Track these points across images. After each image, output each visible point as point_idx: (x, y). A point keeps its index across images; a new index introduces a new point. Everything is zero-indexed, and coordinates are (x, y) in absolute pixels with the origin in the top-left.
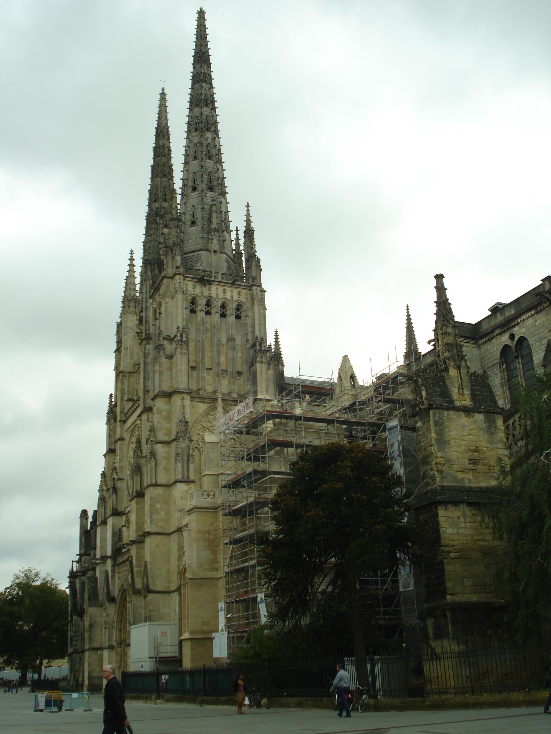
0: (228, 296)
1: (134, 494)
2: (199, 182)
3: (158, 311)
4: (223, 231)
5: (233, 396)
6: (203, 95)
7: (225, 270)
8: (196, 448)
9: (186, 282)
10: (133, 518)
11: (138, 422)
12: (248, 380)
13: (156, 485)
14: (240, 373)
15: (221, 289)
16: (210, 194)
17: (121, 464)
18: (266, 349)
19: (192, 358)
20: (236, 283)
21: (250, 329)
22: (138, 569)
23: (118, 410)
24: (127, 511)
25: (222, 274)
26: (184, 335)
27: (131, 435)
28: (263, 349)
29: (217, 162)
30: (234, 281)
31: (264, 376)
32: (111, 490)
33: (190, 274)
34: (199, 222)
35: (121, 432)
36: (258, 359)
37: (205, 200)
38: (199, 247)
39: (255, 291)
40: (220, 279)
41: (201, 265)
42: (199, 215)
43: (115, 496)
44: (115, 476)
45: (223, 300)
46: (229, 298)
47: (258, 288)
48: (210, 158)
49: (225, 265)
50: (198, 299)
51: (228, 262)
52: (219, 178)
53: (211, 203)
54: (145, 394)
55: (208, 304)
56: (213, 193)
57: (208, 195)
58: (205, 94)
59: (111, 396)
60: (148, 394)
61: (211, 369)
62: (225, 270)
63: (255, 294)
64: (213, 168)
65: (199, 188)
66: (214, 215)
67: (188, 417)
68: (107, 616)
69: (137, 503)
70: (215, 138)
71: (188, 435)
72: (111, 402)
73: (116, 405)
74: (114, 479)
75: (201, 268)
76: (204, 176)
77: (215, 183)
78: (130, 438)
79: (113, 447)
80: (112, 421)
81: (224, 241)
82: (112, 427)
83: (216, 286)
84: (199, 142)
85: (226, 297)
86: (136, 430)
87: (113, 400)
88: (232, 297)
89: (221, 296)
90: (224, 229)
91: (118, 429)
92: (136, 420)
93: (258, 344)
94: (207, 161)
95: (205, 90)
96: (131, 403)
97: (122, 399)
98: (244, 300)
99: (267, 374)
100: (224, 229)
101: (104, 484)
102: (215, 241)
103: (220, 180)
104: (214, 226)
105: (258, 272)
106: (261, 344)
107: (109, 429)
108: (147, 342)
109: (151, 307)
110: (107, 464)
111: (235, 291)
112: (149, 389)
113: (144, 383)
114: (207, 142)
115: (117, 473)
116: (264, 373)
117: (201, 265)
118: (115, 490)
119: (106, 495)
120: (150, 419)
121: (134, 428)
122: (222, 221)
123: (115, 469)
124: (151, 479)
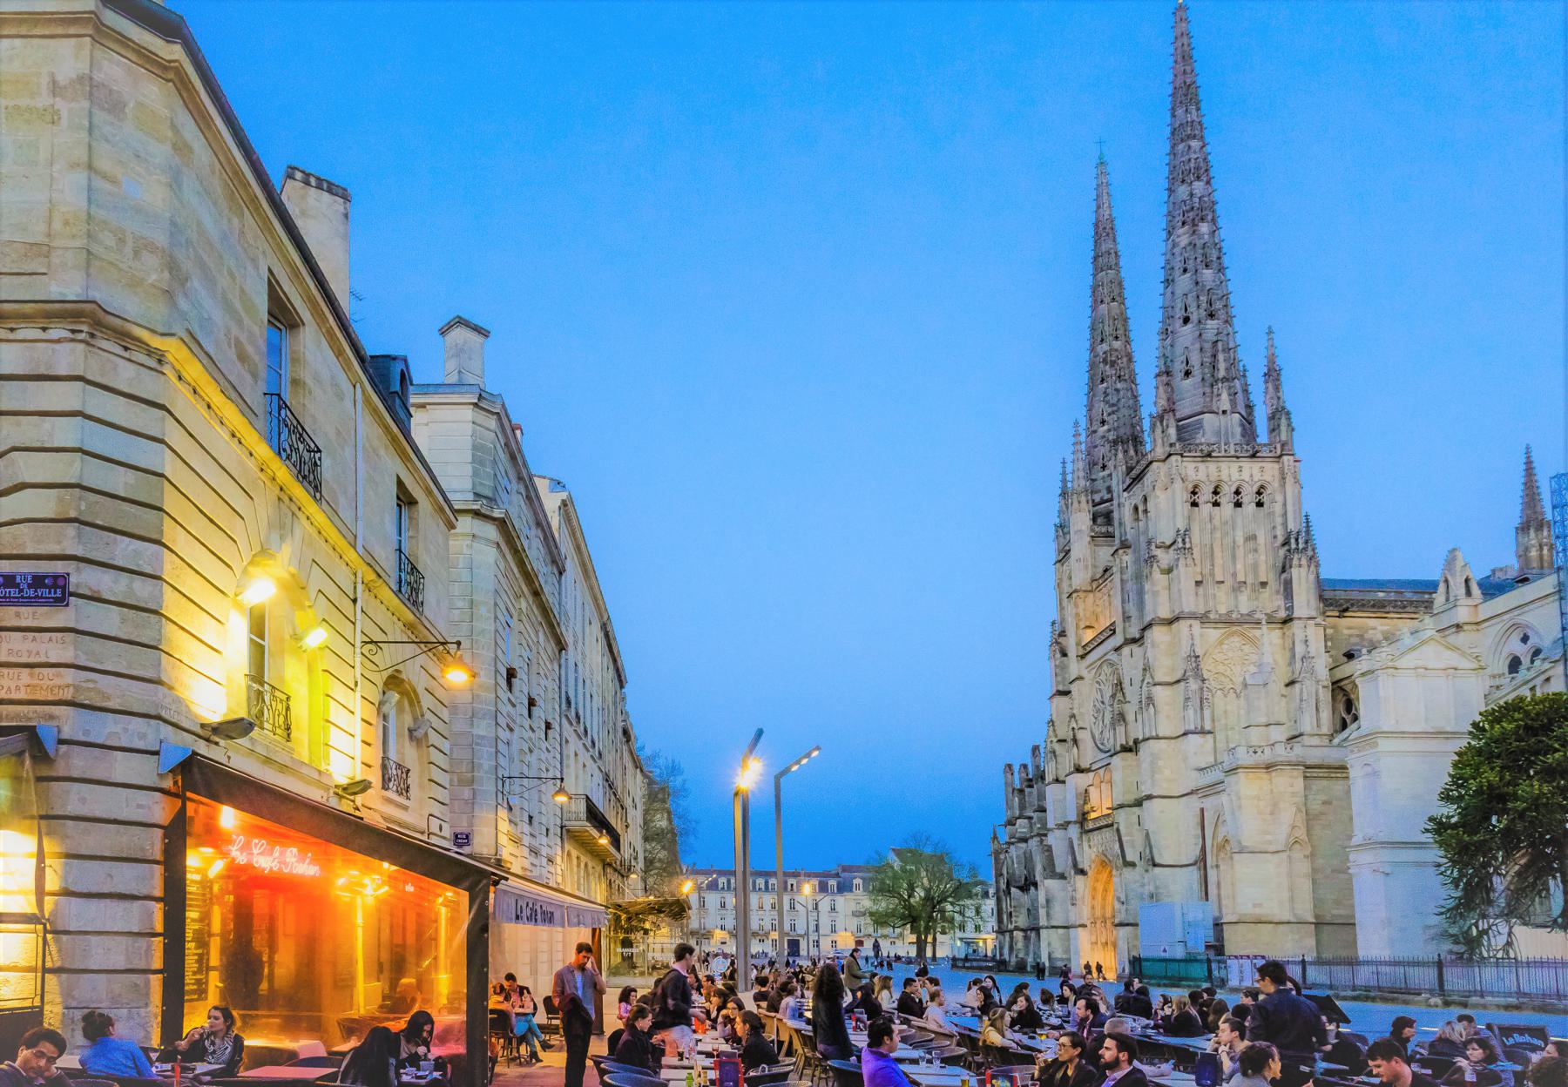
0: (1246, 475)
2: (1192, 309)
5: (1256, 616)
6: (1193, 161)
12: (1278, 592)
13: (1158, 738)
14: (1264, 584)
15: (1234, 466)
16: (1211, 324)
21: (1279, 520)
34: (1196, 371)
37: (1204, 336)
38: (1198, 409)
42: (1195, 360)
50: (1202, 485)
53: (1215, 339)
57: (1208, 327)
58: (1196, 159)
61: (1223, 582)
64: (1214, 281)
65: (1194, 318)
66: (1221, 357)
75: (1203, 440)
76: (1201, 298)
84: (1190, 244)
94: (1204, 271)
114: (1202, 241)
117: (1203, 436)
124: (1150, 731)
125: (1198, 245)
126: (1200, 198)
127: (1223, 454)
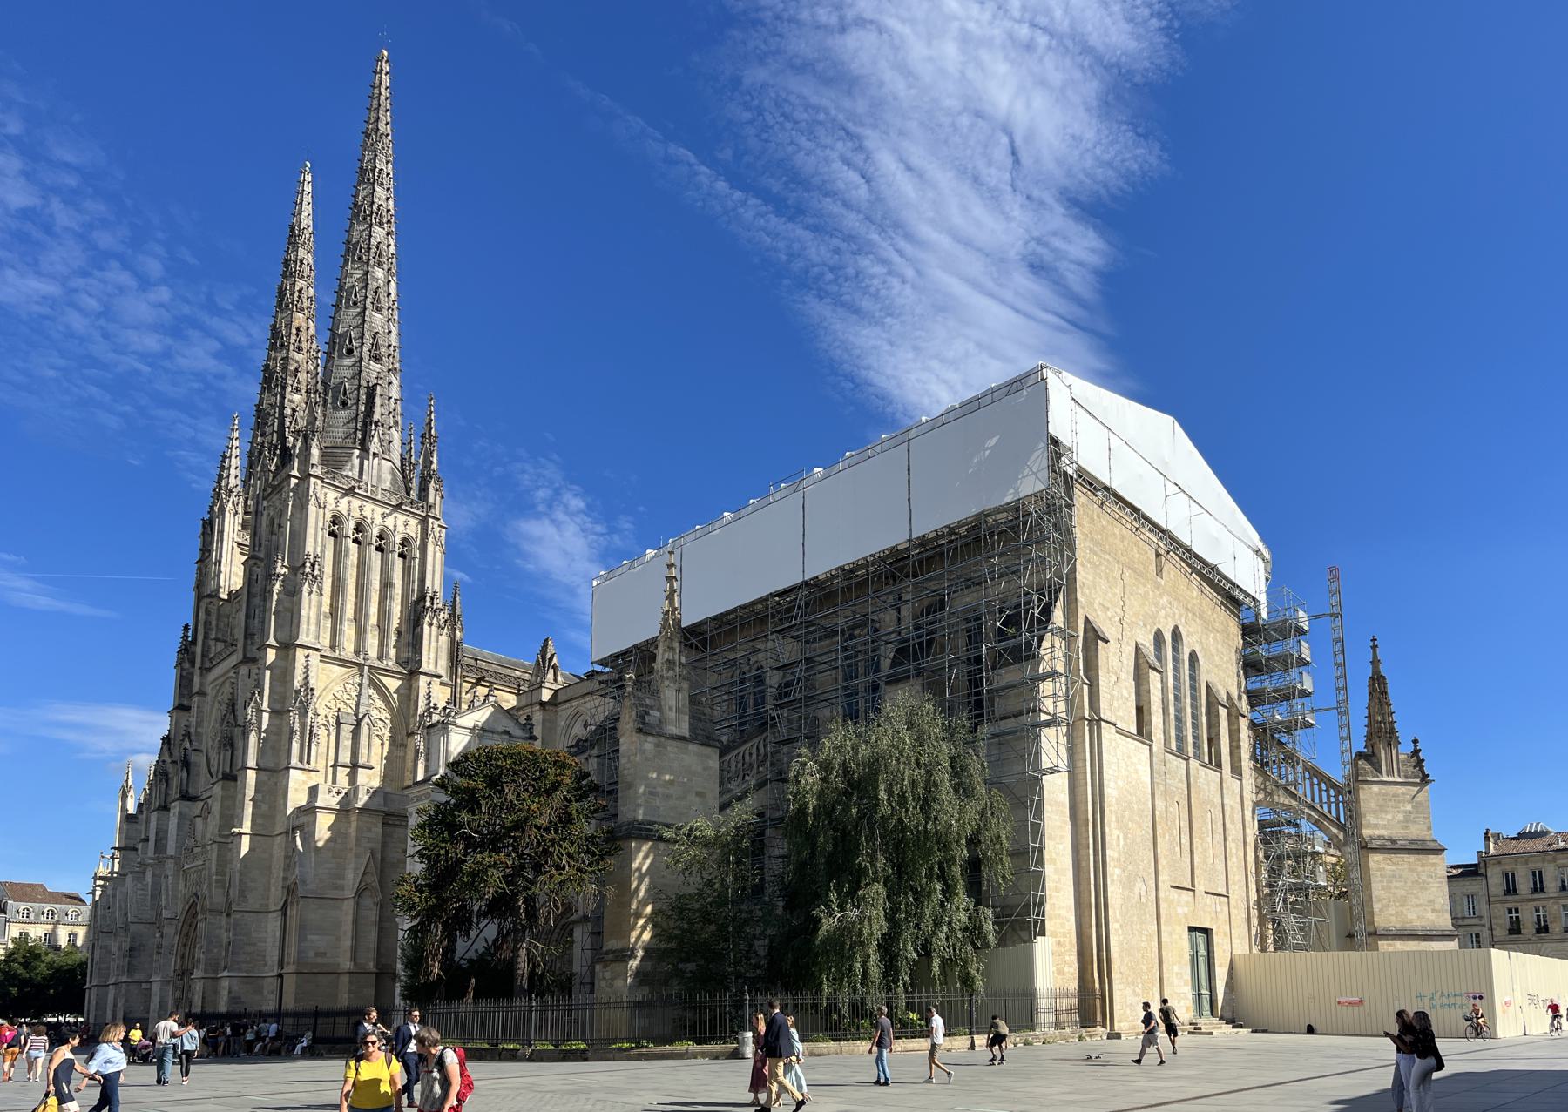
0: (390, 522)
1: (220, 776)
3: (276, 521)
4: (390, 428)
7: (387, 485)
8: (324, 725)
9: (325, 490)
10: (216, 807)
11: (231, 674)
15: (379, 510)
17: (199, 730)
18: (440, 606)
19: (326, 600)
20: (403, 507)
22: (219, 877)
23: (199, 649)
24: (204, 797)
25: (382, 489)
26: (317, 567)
27: (219, 690)
28: (435, 606)
29: (389, 320)
30: (401, 504)
31: (433, 644)
32: (180, 764)
33: (333, 479)
35: (202, 684)
36: (427, 619)
39: (430, 526)
40: (379, 498)
41: (351, 470)
43: (185, 774)
44: (188, 746)
45: (381, 528)
46: (392, 528)
47: (436, 523)
48: (378, 310)
49: (389, 478)
51: (394, 475)
52: (390, 346)
54: (246, 638)
55: (358, 529)
56: (379, 366)
59: (186, 628)
60: (252, 638)
62: (387, 485)
63: (430, 529)
66: (378, 401)
67: (312, 682)
68: (162, 936)
69: (223, 788)
70: (389, 281)
71: (312, 706)
72: (185, 637)
73: (194, 642)
74: (185, 749)
77: (383, 351)
78: (216, 696)
79: (185, 702)
80: (187, 665)
81: (390, 442)
82: (184, 673)
83: (373, 506)
85: (386, 524)
86: (228, 685)
87: (190, 634)
88: (395, 526)
89: (378, 520)
90: (392, 424)
91: (197, 680)
92: (228, 671)
93: (428, 599)
95: (380, 199)
96: (220, 646)
97: (206, 637)
98: (414, 535)
99: (437, 641)
100: (392, 424)
101: (167, 754)
102: (376, 439)
103: (392, 348)
104: (376, 417)
105: (438, 498)
106: (432, 599)
107: (181, 676)
108: (255, 564)
109: (265, 513)
110: (175, 724)
111: (401, 518)
112: (255, 631)
113: (246, 622)
115: (190, 741)
116: (433, 639)
118: (186, 764)
119: (170, 768)
120: (254, 676)
121: (224, 682)
122: (390, 413)
123: (188, 734)
125: (370, 287)
126: (379, 243)
127: (369, 494)
